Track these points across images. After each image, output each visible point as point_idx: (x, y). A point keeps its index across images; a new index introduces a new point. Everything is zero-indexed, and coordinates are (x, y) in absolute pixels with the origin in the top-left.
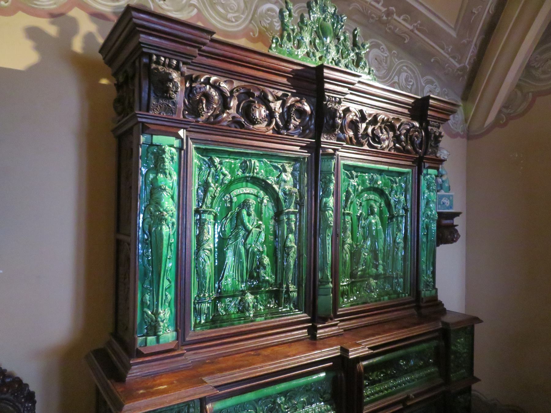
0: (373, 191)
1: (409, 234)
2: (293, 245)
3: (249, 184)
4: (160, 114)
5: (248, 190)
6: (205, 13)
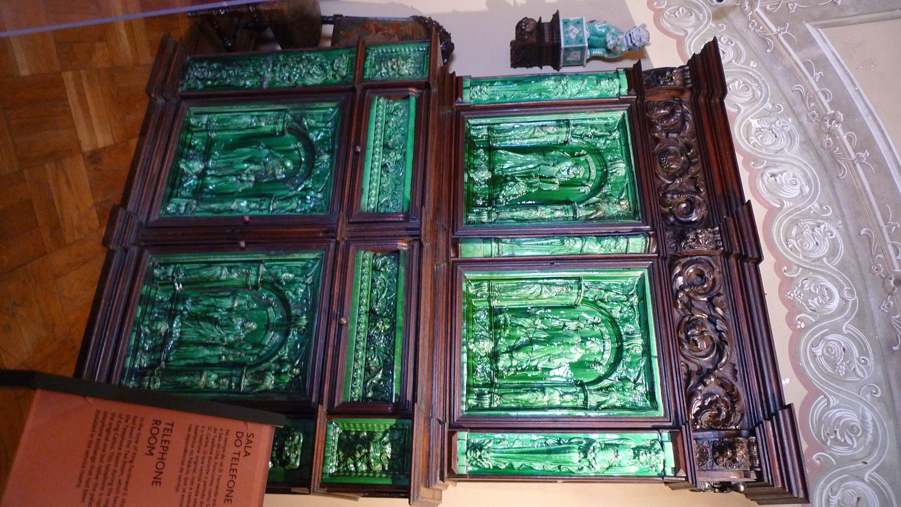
0: (617, 348)
3: (600, 173)
5: (593, 171)
6: (780, 216)
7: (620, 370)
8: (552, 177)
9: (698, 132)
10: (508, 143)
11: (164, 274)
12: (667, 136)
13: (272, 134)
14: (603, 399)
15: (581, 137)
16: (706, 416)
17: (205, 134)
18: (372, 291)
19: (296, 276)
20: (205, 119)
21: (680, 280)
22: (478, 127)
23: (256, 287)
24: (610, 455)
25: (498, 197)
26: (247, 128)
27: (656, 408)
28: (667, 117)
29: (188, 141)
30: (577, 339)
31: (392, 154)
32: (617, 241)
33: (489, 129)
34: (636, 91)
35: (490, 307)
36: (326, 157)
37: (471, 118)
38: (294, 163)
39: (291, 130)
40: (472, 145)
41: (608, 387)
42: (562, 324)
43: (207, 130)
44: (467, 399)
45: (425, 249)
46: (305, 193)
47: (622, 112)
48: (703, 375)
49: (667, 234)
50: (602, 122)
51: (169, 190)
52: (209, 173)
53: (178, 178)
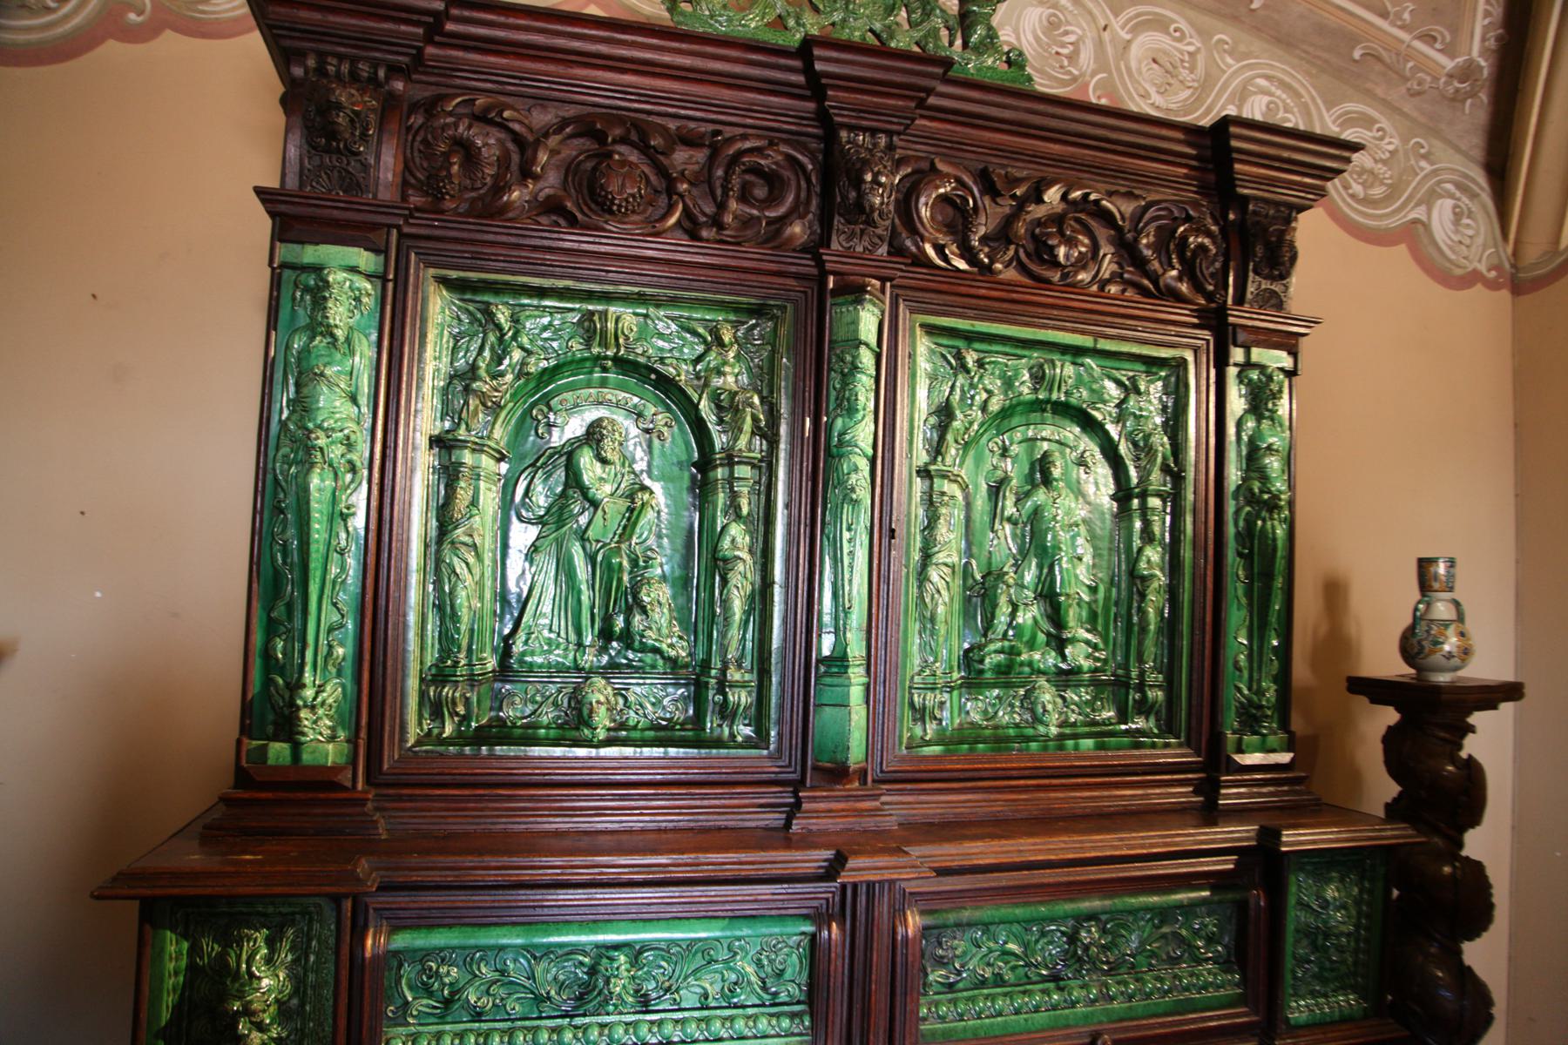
0: (1054, 412)
1: (1187, 553)
2: (745, 555)
4: (330, 191)
37: (403, 740)
41: (1135, 444)
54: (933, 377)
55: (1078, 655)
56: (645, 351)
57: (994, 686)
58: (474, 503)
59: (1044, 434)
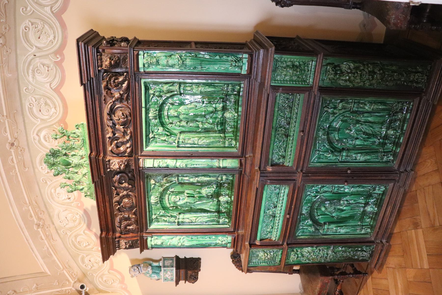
0: (161, 111)
7: (161, 102)
8: (188, 197)
9: (113, 217)
10: (209, 214)
11: (388, 157)
12: (129, 216)
13: (330, 223)
14: (171, 88)
15: (172, 216)
16: (121, 79)
17: (364, 224)
18: (286, 146)
19: (323, 155)
20: (363, 232)
21: (128, 145)
22: (225, 222)
23: (343, 149)
24: (171, 62)
25: (217, 187)
26: (342, 226)
27: (145, 83)
28: (129, 225)
29: (372, 221)
30: (181, 117)
31: (271, 213)
32: (159, 166)
33: (219, 222)
34: (143, 239)
35: (224, 134)
36: (304, 212)
37: (228, 228)
38: (320, 209)
39: (320, 225)
40: (228, 214)
42: (188, 124)
43: (363, 226)
44: (240, 89)
45: (258, 166)
46: (316, 194)
47: (151, 228)
48: (121, 99)
49: (134, 168)
50: (160, 223)
51: (383, 198)
52: (363, 205)
53: (378, 203)
54: (156, 142)
55: (220, 106)
56: (157, 194)
57: (225, 126)
58: (188, 218)
59: (166, 114)
